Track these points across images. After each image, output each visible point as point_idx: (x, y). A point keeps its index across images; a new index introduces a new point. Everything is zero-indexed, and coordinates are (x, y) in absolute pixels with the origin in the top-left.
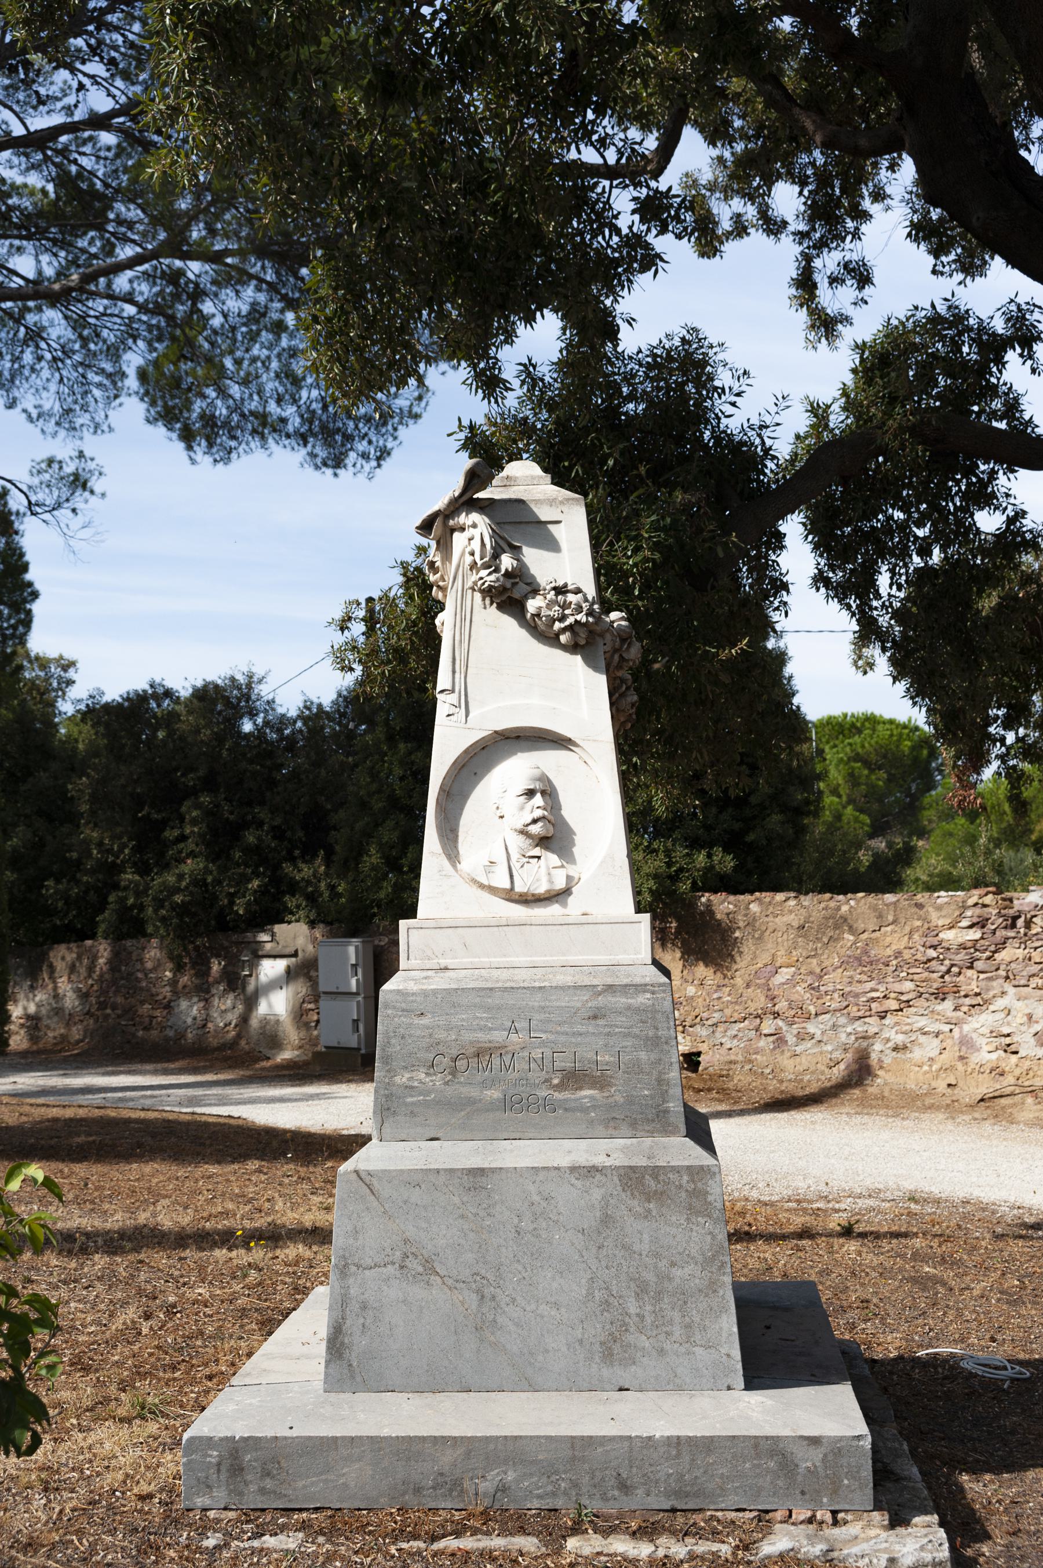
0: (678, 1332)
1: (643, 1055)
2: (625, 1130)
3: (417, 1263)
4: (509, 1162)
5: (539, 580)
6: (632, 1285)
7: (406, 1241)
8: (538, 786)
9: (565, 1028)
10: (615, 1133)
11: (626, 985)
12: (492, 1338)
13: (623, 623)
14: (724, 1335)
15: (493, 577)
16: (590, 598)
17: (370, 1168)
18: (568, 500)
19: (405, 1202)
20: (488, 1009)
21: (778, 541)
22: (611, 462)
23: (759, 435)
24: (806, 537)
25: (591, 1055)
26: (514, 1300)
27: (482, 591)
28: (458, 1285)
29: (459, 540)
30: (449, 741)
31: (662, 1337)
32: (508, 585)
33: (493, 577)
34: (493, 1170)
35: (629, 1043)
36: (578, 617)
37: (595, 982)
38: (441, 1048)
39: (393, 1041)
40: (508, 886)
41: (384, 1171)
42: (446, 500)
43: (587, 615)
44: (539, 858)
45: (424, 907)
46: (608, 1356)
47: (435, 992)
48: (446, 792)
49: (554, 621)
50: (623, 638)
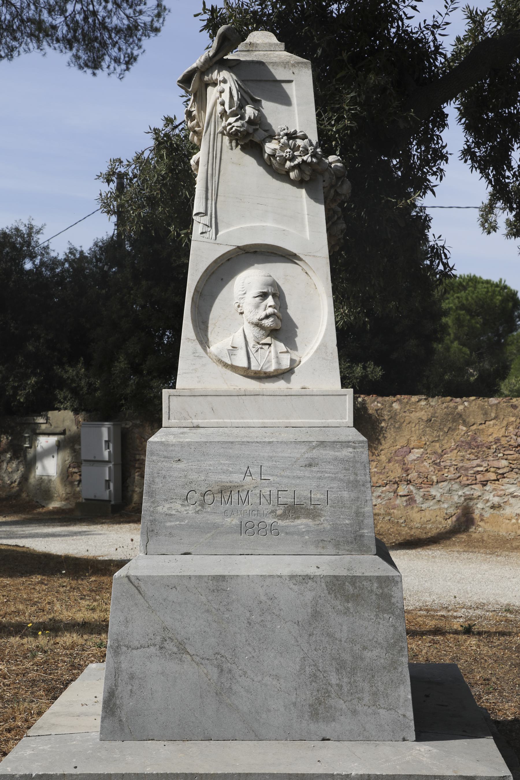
0: (367, 698)
1: (345, 494)
2: (331, 549)
3: (172, 645)
4: (243, 572)
5: (274, 127)
6: (334, 663)
7: (165, 629)
8: (270, 290)
9: (288, 473)
10: (323, 551)
11: (334, 442)
12: (228, 701)
13: (339, 164)
14: (402, 700)
15: (239, 124)
16: (314, 143)
17: (138, 574)
18: (298, 63)
19: (165, 600)
20: (230, 457)
21: (441, 121)
22: (319, 52)
23: (433, 33)
24: (460, 119)
25: (307, 493)
26: (245, 673)
27: (230, 135)
28: (203, 662)
29: (212, 93)
30: (203, 252)
31: (355, 702)
32: (251, 131)
33: (239, 124)
34: (232, 577)
35: (335, 484)
36: (305, 158)
37: (311, 439)
38: (194, 486)
39: (157, 480)
40: (245, 364)
41: (149, 577)
42: (202, 59)
43: (312, 156)
44: (270, 345)
45: (181, 381)
46: (315, 715)
47: (189, 444)
48: (199, 292)
49: (285, 160)
50: (338, 175)
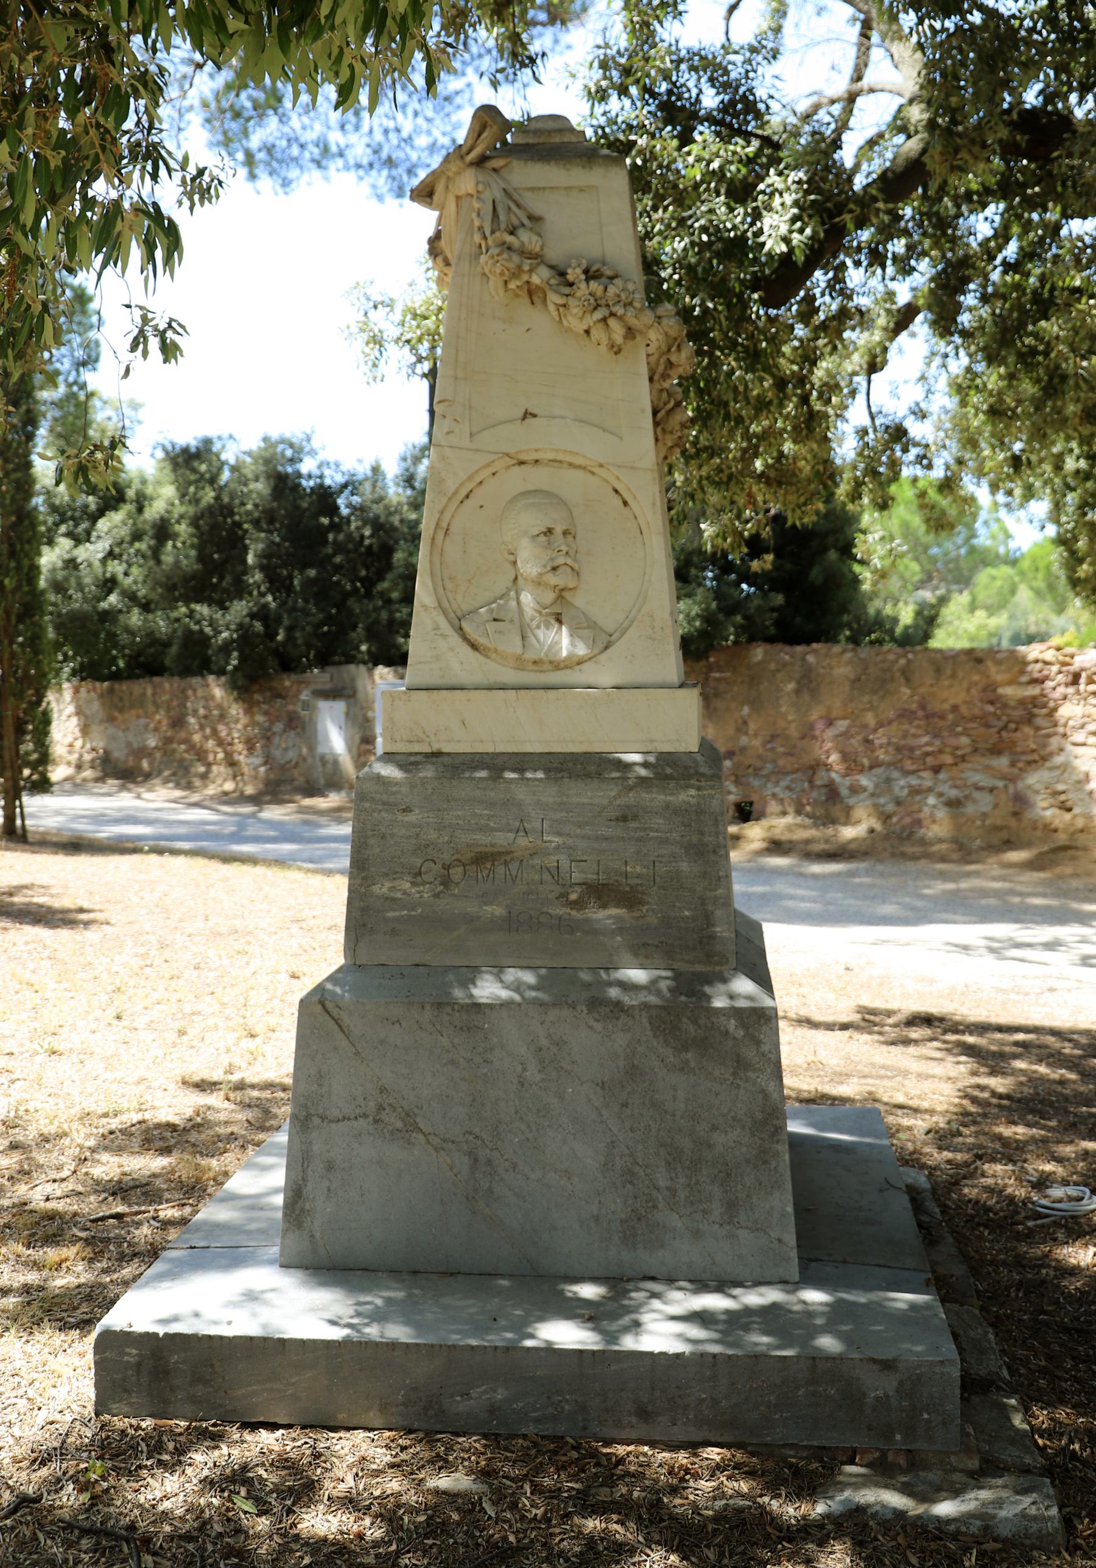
0: (717, 1210)
1: (684, 866)
7: (383, 1090)
9: (588, 831)
19: (382, 1042)
20: (491, 804)
26: (515, 1166)
